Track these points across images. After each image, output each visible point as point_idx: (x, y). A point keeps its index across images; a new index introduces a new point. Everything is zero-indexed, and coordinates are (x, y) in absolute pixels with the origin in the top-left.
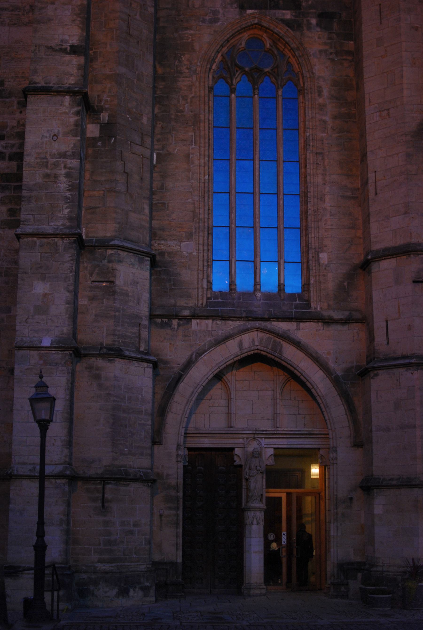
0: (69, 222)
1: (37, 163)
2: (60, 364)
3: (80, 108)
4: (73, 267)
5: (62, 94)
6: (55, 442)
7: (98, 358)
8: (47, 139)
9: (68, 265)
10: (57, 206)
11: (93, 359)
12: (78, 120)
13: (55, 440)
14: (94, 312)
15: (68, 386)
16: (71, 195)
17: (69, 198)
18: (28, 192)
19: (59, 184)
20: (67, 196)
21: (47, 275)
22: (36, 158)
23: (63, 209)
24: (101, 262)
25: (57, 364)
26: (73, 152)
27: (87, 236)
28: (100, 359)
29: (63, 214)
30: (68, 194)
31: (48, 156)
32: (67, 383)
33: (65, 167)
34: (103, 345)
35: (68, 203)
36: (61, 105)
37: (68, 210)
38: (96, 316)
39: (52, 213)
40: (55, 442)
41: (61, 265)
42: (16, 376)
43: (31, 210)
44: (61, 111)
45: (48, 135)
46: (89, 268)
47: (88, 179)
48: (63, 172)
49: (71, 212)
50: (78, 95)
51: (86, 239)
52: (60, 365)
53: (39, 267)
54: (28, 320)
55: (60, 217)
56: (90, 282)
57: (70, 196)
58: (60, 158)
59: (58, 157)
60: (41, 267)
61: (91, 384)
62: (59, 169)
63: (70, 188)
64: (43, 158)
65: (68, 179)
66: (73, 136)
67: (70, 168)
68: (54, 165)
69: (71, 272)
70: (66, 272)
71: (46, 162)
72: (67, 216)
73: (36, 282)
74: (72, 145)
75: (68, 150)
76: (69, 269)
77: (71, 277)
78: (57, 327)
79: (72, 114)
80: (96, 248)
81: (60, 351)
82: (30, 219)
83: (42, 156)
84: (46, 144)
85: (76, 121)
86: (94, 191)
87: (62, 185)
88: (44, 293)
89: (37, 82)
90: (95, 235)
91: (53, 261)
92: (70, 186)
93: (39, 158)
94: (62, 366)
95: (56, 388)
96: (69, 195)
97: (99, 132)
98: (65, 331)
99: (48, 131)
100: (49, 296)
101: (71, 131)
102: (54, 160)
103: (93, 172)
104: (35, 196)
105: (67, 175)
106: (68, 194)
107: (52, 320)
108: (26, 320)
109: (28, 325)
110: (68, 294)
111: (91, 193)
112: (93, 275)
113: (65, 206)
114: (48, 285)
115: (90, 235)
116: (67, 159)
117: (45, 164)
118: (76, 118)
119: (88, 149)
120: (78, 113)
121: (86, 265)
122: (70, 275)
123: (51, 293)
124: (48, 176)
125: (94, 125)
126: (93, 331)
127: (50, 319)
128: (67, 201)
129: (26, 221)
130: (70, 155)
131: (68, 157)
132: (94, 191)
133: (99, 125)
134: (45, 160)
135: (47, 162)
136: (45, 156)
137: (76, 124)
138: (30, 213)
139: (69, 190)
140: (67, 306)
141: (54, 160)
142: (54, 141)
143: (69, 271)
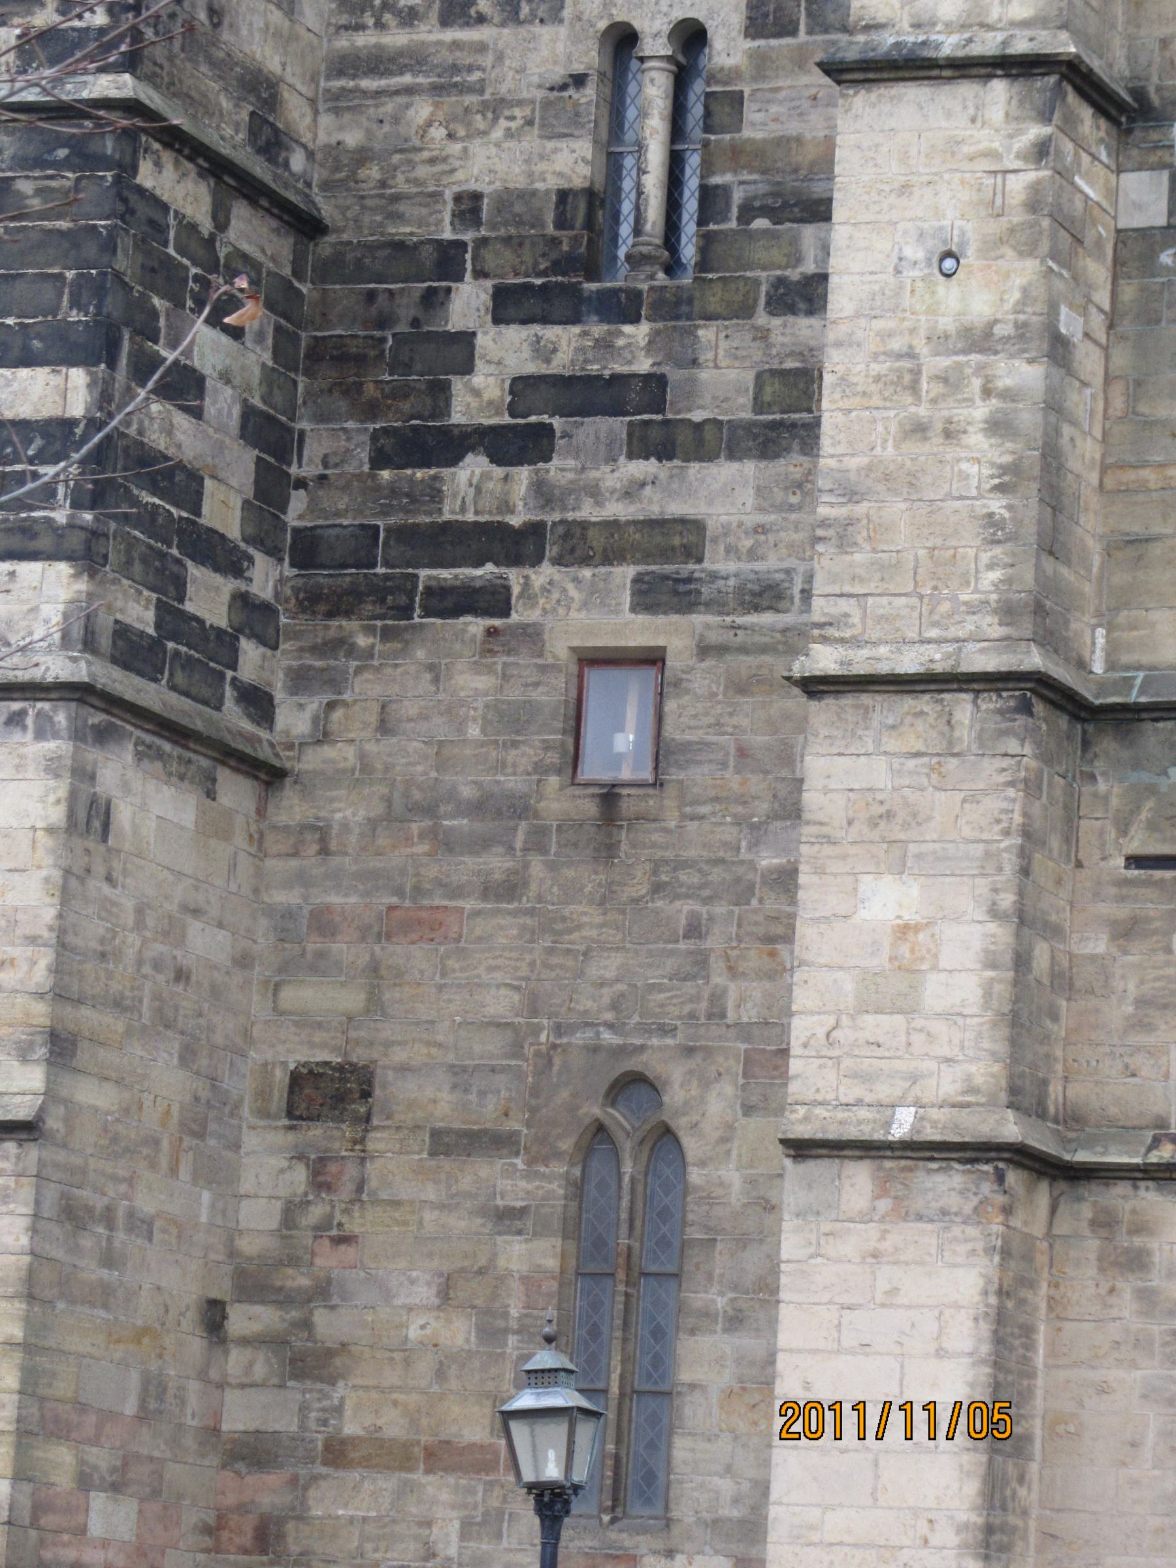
0: (1000, 624)
1: (877, 379)
2: (956, 1214)
3: (1048, 130)
4: (1012, 811)
5: (974, 71)
6: (932, 1530)
7: (1142, 1184)
8: (916, 273)
9: (993, 804)
10: (954, 556)
11: (1122, 1188)
12: (1039, 182)
13: (931, 1521)
14: (1131, 987)
15: (987, 1305)
16: (1009, 508)
17: (1004, 519)
18: (842, 500)
19: (964, 466)
20: (991, 515)
21: (913, 848)
22: (875, 357)
23: (977, 571)
24: (1166, 774)
25: (944, 1212)
26: (1017, 325)
27: (1111, 666)
28: (1147, 1189)
29: (976, 591)
30: (997, 505)
31: (922, 349)
32: (985, 1293)
33: (987, 392)
34: (1168, 1128)
35: (999, 542)
36: (973, 120)
37: (995, 575)
38: (1142, 1002)
39: (935, 588)
40: (932, 1530)
41: (967, 805)
42: (788, 1261)
43: (853, 579)
44: (973, 149)
45: (920, 255)
46: (1114, 802)
47: (1119, 414)
48: (981, 411)
49: (1008, 581)
50: (1044, 75)
51: (1109, 675)
52: (959, 1219)
53: (881, 817)
54: (834, 1034)
55: (966, 603)
56: (1121, 862)
57: (1007, 515)
58: (965, 352)
59: (959, 346)
60: (889, 815)
61: (1112, 1290)
62: (965, 400)
63: (1006, 478)
64: (900, 356)
65: (1000, 441)
66: (1021, 254)
67: (1007, 395)
68: (946, 381)
69: (1006, 833)
70: (985, 836)
71: (911, 371)
72: (994, 597)
73: (868, 878)
74: (1017, 295)
75: (999, 316)
76: (998, 821)
77: (1005, 855)
78: (948, 1060)
79: (1018, 157)
80: (1144, 715)
81: (959, 1161)
82: (846, 615)
83: (896, 345)
84: (913, 291)
85: (1035, 189)
86: (1143, 467)
87: (976, 468)
88: (900, 922)
89: (883, 21)
90: (1145, 659)
91: (936, 788)
92: (1004, 469)
93: (884, 353)
94: (964, 1223)
95: (941, 1313)
96: (1003, 511)
97: (1163, 206)
98: (979, 1080)
99: (921, 235)
100: (921, 936)
101: (1012, 231)
102: (945, 362)
103: (1138, 384)
104: (868, 516)
105: (997, 426)
106: (997, 505)
107: (928, 1034)
108: (828, 1035)
109: (836, 1052)
110: (992, 927)
111: (1130, 476)
112: (1132, 833)
113: (985, 557)
114: (915, 891)
115: (1126, 658)
116: (996, 353)
117: (907, 378)
118: (1032, 176)
119: (1122, 282)
120: (1041, 151)
121: (1102, 786)
122: (1003, 845)
123: (927, 925)
124: (919, 429)
125: (1145, 175)
126: (1127, 1066)
127: (921, 1030)
128: (994, 534)
129: (831, 624)
130: (1009, 338)
131: (999, 347)
132: (1143, 465)
133: (1165, 176)
134: (907, 364)
135: (916, 373)
136: (911, 347)
137: (1033, 205)
138: (847, 589)
139: (1000, 488)
140: (990, 974)
141: (945, 362)
142: (943, 278)
143: (997, 828)
